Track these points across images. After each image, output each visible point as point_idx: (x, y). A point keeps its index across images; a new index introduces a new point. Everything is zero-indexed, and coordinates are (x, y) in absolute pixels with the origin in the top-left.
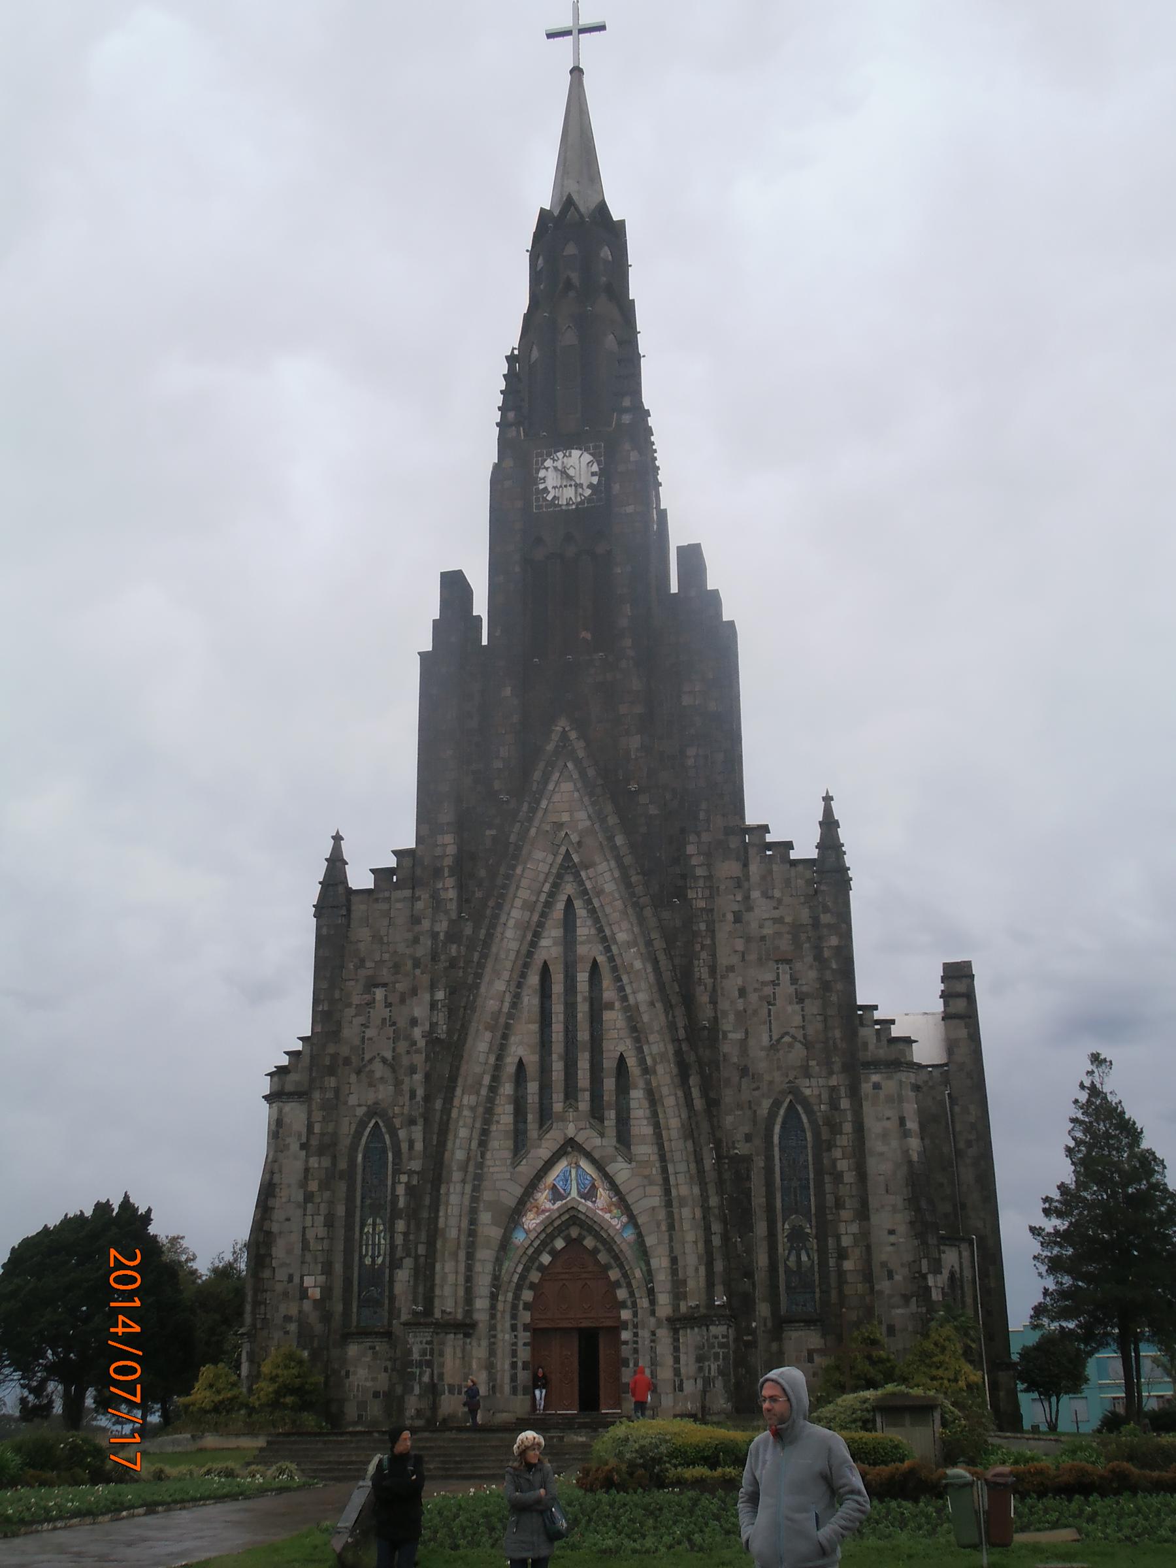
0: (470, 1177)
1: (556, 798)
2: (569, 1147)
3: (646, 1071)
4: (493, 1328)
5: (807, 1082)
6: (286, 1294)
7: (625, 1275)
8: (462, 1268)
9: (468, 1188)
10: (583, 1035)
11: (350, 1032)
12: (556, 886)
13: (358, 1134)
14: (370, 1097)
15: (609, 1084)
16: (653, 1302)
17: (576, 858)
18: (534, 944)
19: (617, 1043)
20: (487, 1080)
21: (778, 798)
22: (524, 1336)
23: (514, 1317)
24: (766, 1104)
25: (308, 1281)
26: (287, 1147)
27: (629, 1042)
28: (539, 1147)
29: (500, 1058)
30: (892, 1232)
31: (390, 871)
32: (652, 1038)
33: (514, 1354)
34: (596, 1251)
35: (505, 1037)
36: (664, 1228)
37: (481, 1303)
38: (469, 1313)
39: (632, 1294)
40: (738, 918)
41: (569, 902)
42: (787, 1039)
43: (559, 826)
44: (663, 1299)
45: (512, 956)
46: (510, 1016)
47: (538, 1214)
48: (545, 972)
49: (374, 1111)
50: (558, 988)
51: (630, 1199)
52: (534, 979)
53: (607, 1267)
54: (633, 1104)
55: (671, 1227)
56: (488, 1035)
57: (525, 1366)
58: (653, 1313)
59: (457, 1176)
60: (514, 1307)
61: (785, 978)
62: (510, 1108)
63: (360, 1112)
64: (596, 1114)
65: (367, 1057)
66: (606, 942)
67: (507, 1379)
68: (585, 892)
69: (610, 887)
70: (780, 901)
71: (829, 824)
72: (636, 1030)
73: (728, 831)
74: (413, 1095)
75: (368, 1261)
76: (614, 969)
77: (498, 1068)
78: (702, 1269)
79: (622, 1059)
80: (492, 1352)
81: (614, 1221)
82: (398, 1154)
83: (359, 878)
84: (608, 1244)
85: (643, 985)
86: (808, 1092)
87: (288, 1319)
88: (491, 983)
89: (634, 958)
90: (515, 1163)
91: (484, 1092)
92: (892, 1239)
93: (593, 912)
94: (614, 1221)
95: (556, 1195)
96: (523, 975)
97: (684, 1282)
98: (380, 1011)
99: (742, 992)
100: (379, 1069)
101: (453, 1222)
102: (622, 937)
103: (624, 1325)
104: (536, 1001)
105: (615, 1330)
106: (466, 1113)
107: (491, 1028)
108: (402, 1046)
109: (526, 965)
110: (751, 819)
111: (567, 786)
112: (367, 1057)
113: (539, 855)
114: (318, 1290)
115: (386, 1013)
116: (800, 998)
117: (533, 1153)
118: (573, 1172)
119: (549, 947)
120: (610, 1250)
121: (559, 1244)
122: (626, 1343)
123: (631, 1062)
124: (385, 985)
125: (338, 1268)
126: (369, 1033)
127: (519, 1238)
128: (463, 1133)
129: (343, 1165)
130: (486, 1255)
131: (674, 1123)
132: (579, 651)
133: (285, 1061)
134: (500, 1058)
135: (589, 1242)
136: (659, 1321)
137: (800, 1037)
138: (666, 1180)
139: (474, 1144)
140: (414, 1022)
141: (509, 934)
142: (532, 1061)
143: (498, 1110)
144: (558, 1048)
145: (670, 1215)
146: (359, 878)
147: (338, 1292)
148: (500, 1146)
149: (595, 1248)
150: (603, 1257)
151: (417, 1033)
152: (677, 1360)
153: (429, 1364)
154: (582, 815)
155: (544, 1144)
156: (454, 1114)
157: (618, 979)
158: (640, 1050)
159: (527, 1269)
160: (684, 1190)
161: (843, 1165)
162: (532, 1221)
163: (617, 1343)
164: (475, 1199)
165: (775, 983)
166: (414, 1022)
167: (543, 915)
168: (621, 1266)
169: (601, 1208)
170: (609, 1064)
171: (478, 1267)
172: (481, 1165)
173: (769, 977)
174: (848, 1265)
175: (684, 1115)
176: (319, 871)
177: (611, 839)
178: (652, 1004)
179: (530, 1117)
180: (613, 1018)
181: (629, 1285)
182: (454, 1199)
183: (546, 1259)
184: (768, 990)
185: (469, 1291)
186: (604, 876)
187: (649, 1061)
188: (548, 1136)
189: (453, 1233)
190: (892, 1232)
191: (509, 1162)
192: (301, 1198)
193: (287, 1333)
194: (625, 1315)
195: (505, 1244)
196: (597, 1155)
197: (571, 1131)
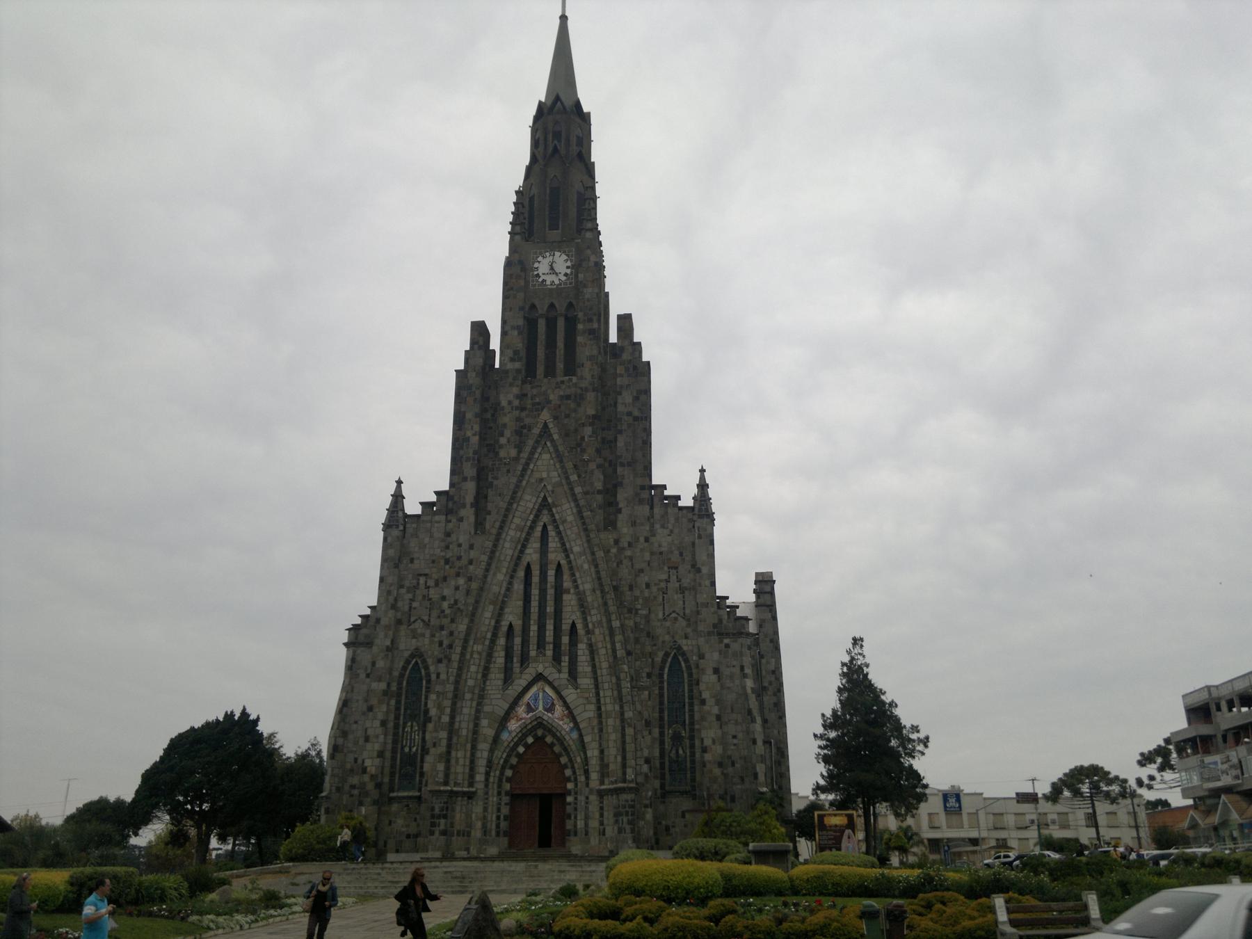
0: (476, 697)
1: (539, 463)
2: (540, 677)
3: (588, 632)
4: (487, 793)
5: (684, 642)
6: (352, 770)
7: (571, 760)
8: (468, 754)
9: (474, 704)
10: (550, 609)
11: (403, 605)
12: (537, 516)
13: (404, 668)
14: (414, 643)
15: (565, 640)
16: (587, 778)
17: (550, 500)
18: (522, 552)
19: (571, 613)
20: (489, 635)
21: (673, 472)
22: (506, 799)
23: (500, 786)
24: (661, 654)
25: (368, 763)
26: (358, 675)
27: (578, 614)
29: (498, 622)
30: (734, 737)
31: (432, 504)
32: (593, 612)
33: (499, 810)
34: (553, 745)
35: (502, 609)
37: (480, 778)
39: (574, 773)
40: (647, 540)
41: (545, 526)
42: (674, 615)
43: (541, 480)
44: (594, 776)
45: (508, 558)
46: (505, 596)
47: (518, 720)
48: (528, 569)
49: (417, 653)
50: (535, 579)
52: (521, 573)
53: (560, 755)
54: (580, 652)
55: (601, 730)
56: (491, 607)
57: (506, 818)
58: (587, 785)
59: (468, 696)
60: (500, 780)
61: (674, 578)
62: (503, 654)
63: (407, 654)
66: (566, 552)
67: (494, 827)
68: (555, 521)
69: (570, 518)
70: (671, 531)
71: (703, 486)
73: (643, 488)
74: (441, 644)
75: (407, 750)
76: (571, 568)
78: (619, 759)
80: (485, 809)
81: (565, 726)
82: (429, 681)
83: (412, 507)
84: (561, 741)
85: (589, 579)
86: (685, 648)
87: (353, 787)
88: (495, 574)
89: (583, 563)
90: (505, 689)
91: (487, 643)
92: (735, 741)
93: (559, 533)
94: (565, 726)
95: (529, 709)
96: (514, 571)
97: (607, 766)
99: (648, 586)
100: (419, 625)
101: (464, 725)
102: (576, 549)
103: (569, 793)
104: (522, 587)
105: (563, 796)
108: (435, 613)
109: (516, 565)
110: (656, 480)
111: (546, 456)
113: (527, 497)
116: (682, 590)
117: (517, 682)
119: (532, 555)
120: (562, 744)
121: (530, 740)
123: (579, 626)
124: (426, 575)
125: (388, 755)
126: (415, 604)
127: (505, 736)
128: (473, 668)
129: (394, 687)
130: (484, 747)
131: (605, 665)
132: (557, 373)
133: (359, 621)
134: (498, 622)
135: (549, 739)
136: (591, 791)
138: (598, 701)
139: (480, 676)
140: (444, 598)
141: (507, 545)
142: (518, 624)
143: (496, 654)
145: (600, 723)
146: (412, 507)
147: (387, 771)
148: (496, 677)
150: (557, 749)
151: (445, 605)
152: (602, 815)
153: (445, 817)
154: (555, 474)
155: (524, 676)
156: (468, 657)
157: (573, 575)
158: (585, 619)
159: (509, 756)
161: (706, 695)
162: (513, 725)
163: (564, 803)
164: (478, 711)
165: (667, 581)
166: (444, 598)
167: (529, 534)
168: (568, 754)
169: (557, 717)
170: (566, 627)
171: (479, 754)
172: (483, 690)
173: (664, 577)
174: (708, 757)
175: (611, 660)
176: (387, 501)
178: (594, 590)
179: (515, 660)
180: (569, 600)
181: (573, 767)
182: (466, 711)
183: (521, 749)
184: (663, 585)
185: (472, 769)
186: (566, 510)
187: (590, 626)
189: (464, 732)
190: (734, 737)
192: (365, 708)
193: (352, 796)
194: (570, 786)
195: (496, 740)
196: (556, 684)
197: (540, 669)
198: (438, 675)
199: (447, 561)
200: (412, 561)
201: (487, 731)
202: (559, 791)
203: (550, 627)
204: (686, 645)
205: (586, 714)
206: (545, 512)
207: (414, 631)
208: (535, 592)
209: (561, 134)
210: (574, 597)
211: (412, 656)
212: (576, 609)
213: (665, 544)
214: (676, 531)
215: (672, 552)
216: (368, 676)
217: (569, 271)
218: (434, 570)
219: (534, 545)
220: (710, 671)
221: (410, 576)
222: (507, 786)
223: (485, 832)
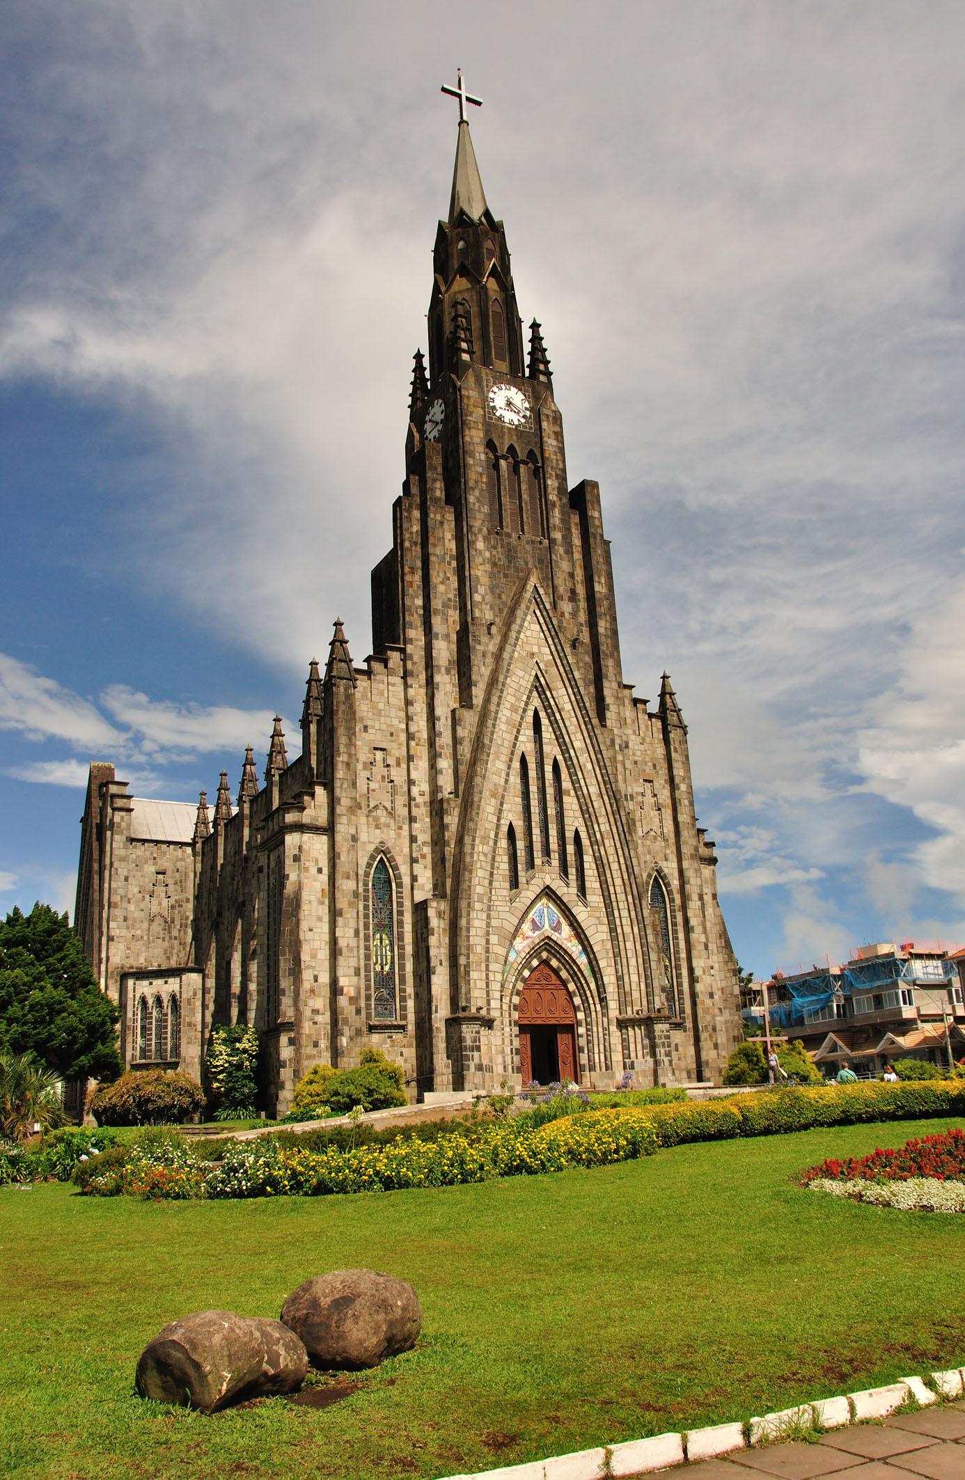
13: (369, 865)
14: (377, 836)
15: (570, 849)
19: (574, 821)
20: (492, 835)
26: (306, 869)
27: (581, 820)
29: (499, 819)
35: (502, 804)
36: (611, 955)
37: (495, 1004)
39: (585, 1000)
49: (382, 850)
50: (532, 773)
52: (516, 764)
56: (493, 801)
59: (478, 906)
63: (371, 848)
69: (568, 707)
70: (644, 739)
71: (665, 693)
72: (586, 811)
77: (498, 826)
79: (577, 832)
81: (574, 948)
82: (400, 885)
86: (666, 871)
91: (491, 843)
94: (574, 948)
95: (536, 927)
96: (511, 760)
98: (379, 770)
105: (570, 1029)
106: (482, 858)
107: (493, 795)
114: (352, 989)
115: (385, 771)
119: (526, 744)
121: (535, 963)
123: (583, 835)
126: (373, 785)
131: (618, 882)
134: (499, 819)
137: (659, 831)
142: (519, 826)
144: (536, 818)
160: (627, 929)
169: (565, 938)
173: (641, 790)
180: (570, 801)
183: (526, 973)
186: (562, 696)
202: (568, 1022)
203: (553, 832)
204: (670, 868)
205: (599, 936)
207: (376, 819)
208: (533, 788)
209: (469, 251)
213: (638, 753)
214: (648, 740)
215: (646, 763)
216: (320, 871)
217: (528, 414)
218: (394, 745)
219: (528, 732)
220: (695, 897)
221: (366, 749)
222: (516, 1015)
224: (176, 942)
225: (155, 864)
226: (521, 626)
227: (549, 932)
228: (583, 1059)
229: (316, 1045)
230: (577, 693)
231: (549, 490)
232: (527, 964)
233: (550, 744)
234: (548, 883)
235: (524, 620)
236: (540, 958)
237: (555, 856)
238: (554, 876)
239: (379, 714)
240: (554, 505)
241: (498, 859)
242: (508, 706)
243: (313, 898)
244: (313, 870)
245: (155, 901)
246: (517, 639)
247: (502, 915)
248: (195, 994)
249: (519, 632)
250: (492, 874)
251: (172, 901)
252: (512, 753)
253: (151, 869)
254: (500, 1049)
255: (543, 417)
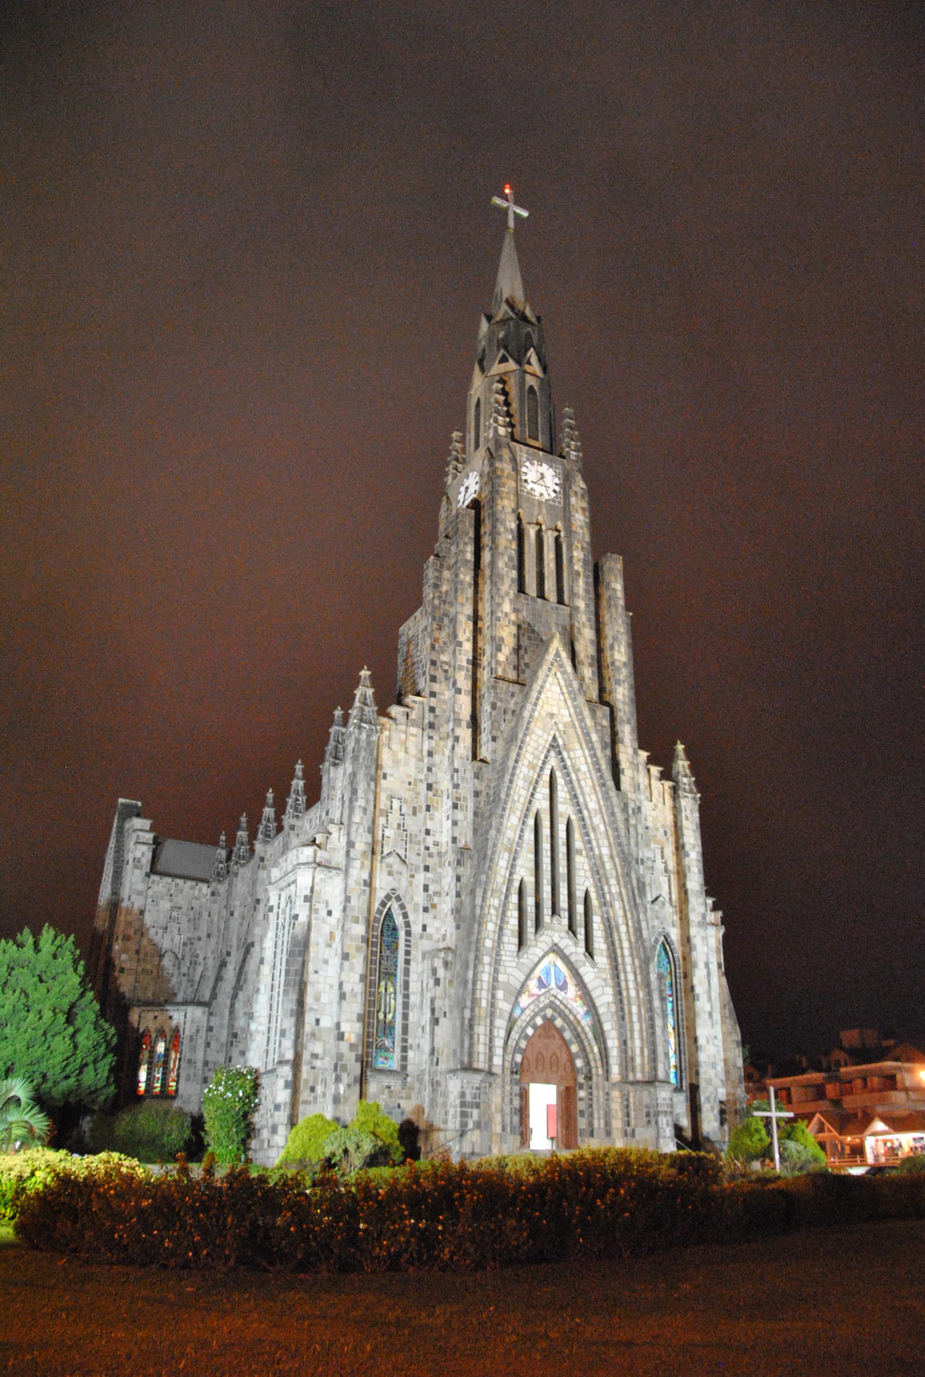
10: (562, 869)
15: (580, 908)
16: (607, 1071)
25: (345, 1027)
26: (317, 911)
28: (536, 946)
29: (511, 874)
35: (515, 859)
38: (490, 1066)
50: (546, 831)
51: (594, 994)
52: (531, 822)
64: (571, 928)
65: (385, 852)
68: (565, 767)
69: (584, 768)
70: (656, 806)
77: (510, 881)
81: (579, 1008)
82: (408, 933)
84: (574, 1026)
95: (541, 984)
96: (526, 816)
112: (385, 852)
117: (531, 950)
118: (552, 968)
121: (539, 1021)
122: (581, 1099)
123: (593, 895)
131: (626, 944)
134: (511, 874)
135: (559, 1022)
142: (530, 880)
149: (563, 1026)
153: (478, 1106)
154: (566, 712)
168: (581, 1043)
172: (498, 954)
177: (587, 735)
180: (581, 862)
186: (579, 757)
188: (541, 939)
191: (515, 954)
193: (313, 1068)
198: (424, 928)
199: (429, 787)
200: (385, 777)
201: (504, 1006)
204: (675, 934)
205: (604, 998)
206: (552, 754)
208: (546, 846)
210: (586, 860)
211: (388, 897)
212: (589, 874)
213: (650, 819)
215: (657, 829)
216: (330, 913)
217: (557, 488)
219: (543, 791)
223: (504, 1129)
224: (184, 979)
225: (171, 900)
226: (542, 687)
227: (555, 991)
228: (582, 1123)
229: (313, 1089)
230: (594, 755)
231: (575, 561)
232: (531, 1022)
233: (564, 803)
234: (556, 941)
235: (545, 682)
236: (544, 1017)
237: (565, 914)
238: (563, 935)
239: (396, 762)
240: (578, 574)
241: (509, 913)
242: (526, 763)
243: (321, 940)
244: (323, 913)
245: (167, 937)
246: (538, 699)
247: (509, 970)
248: (198, 1031)
249: (540, 693)
250: (501, 929)
251: (184, 938)
252: (528, 810)
253: (165, 905)
254: (499, 1107)
255: (572, 494)
